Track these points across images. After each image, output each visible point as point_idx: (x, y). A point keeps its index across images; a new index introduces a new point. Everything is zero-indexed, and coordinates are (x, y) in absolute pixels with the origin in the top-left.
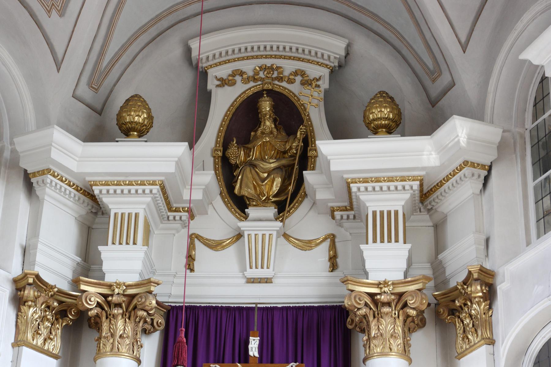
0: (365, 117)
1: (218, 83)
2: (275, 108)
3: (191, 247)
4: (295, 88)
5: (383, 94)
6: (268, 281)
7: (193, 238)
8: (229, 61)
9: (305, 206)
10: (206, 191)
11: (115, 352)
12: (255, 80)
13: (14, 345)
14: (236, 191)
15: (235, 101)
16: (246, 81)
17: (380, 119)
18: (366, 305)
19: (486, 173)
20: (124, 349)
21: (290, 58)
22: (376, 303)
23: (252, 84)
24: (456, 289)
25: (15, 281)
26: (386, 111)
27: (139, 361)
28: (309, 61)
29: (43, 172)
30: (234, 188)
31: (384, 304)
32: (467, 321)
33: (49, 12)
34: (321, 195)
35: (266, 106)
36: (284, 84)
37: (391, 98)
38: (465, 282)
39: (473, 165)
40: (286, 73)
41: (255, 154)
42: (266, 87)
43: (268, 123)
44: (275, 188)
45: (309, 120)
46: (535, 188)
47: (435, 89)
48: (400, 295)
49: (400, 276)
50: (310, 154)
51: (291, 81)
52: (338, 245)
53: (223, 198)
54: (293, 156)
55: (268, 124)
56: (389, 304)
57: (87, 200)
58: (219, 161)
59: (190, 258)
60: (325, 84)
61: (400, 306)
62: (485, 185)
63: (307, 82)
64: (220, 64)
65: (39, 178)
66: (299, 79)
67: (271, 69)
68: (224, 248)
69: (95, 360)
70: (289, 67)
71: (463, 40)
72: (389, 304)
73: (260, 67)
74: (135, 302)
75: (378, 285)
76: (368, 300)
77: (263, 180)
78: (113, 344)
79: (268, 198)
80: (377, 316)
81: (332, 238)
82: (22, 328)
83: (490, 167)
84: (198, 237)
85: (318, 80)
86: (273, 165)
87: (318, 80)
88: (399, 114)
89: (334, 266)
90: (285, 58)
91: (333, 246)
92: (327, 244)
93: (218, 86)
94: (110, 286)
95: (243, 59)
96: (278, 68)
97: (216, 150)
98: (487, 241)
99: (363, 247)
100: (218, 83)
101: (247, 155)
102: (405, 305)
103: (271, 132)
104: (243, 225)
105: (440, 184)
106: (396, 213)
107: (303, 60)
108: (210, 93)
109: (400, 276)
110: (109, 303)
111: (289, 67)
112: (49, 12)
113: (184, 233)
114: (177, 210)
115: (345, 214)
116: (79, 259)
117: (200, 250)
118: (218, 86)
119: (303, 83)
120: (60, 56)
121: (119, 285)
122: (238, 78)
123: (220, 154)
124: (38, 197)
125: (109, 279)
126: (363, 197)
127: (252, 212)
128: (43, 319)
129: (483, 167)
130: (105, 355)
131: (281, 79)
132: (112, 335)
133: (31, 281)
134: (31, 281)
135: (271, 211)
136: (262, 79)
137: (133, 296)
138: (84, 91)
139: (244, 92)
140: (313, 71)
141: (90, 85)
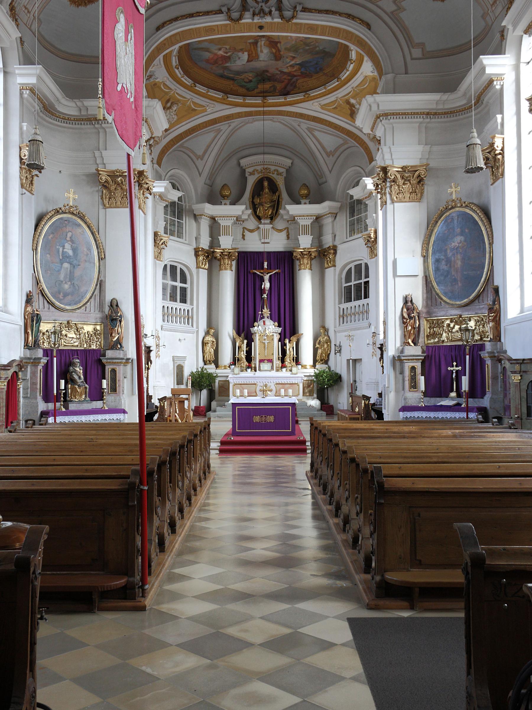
0: (299, 193)
1: (249, 174)
2: (269, 185)
3: (243, 232)
4: (274, 176)
5: (305, 185)
6: (268, 243)
7: (244, 228)
8: (253, 166)
9: (279, 218)
10: (249, 216)
11: (226, 269)
12: (261, 173)
13: (196, 268)
14: (257, 214)
15: (255, 181)
16: (259, 173)
17: (304, 194)
18: (300, 255)
19: (335, 215)
20: (228, 268)
21: (273, 165)
22: (302, 254)
23: (261, 174)
24: (325, 249)
25: (195, 249)
26: (306, 192)
27: (232, 271)
28: (279, 166)
29: (201, 215)
30: (257, 212)
31: (305, 255)
32: (328, 259)
33: (198, 159)
34: (285, 217)
35: (266, 184)
36: (271, 174)
37: (307, 186)
38: (328, 248)
39: (332, 213)
40: (272, 170)
41: (263, 200)
42: (265, 176)
43: (267, 190)
44: (270, 213)
45: (280, 190)
46: (349, 221)
47: (321, 181)
48: (310, 252)
49: (310, 246)
50: (280, 200)
51: (273, 174)
52: (289, 231)
53: (253, 216)
54: (275, 201)
55: (267, 190)
56: (306, 255)
57: (212, 220)
58: (251, 203)
59: (243, 236)
60: (285, 175)
61: (309, 255)
62: (335, 218)
63: (279, 174)
64: (250, 167)
65: (200, 217)
66: (276, 172)
67: (266, 169)
68: (254, 232)
69: (219, 271)
70: (273, 168)
71: (330, 169)
72: (306, 255)
73: (263, 168)
74: (231, 254)
75: (303, 249)
76: (300, 253)
77: (266, 210)
78: (225, 267)
79: (267, 216)
80: (303, 258)
81: (287, 229)
82: (198, 263)
83: (337, 213)
84: (245, 228)
85: (282, 173)
86: (269, 205)
87: (282, 173)
88: (309, 192)
89: (288, 237)
90: (271, 165)
91: (288, 232)
92: (286, 231)
93: (249, 175)
94: (223, 250)
95: (257, 165)
96: (269, 168)
97: (250, 199)
98: (335, 236)
99: (299, 237)
100: (249, 174)
101: (260, 200)
102: (311, 255)
103: (268, 193)
104: (260, 226)
105: (322, 216)
106: (309, 225)
107: (277, 166)
108: (247, 177)
109: (310, 246)
110: (223, 255)
111: (273, 168)
112: (198, 159)
113: (241, 227)
114: (239, 221)
115: (292, 222)
116: (211, 239)
117: (247, 233)
118: (249, 175)
119: (278, 174)
120: (201, 172)
121: (226, 249)
122: (256, 172)
123: (251, 200)
124: (199, 222)
125: (222, 247)
126: (299, 221)
127: (263, 221)
128: (203, 259)
129: (335, 213)
130: (222, 270)
131: (270, 173)
132: (225, 264)
133: (200, 249)
134: (200, 249)
135: (268, 221)
136: (264, 173)
137: (230, 252)
138: (208, 182)
139: (258, 178)
140: (281, 170)
141: (209, 179)
